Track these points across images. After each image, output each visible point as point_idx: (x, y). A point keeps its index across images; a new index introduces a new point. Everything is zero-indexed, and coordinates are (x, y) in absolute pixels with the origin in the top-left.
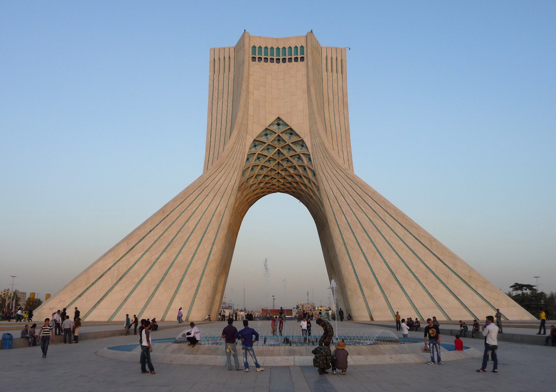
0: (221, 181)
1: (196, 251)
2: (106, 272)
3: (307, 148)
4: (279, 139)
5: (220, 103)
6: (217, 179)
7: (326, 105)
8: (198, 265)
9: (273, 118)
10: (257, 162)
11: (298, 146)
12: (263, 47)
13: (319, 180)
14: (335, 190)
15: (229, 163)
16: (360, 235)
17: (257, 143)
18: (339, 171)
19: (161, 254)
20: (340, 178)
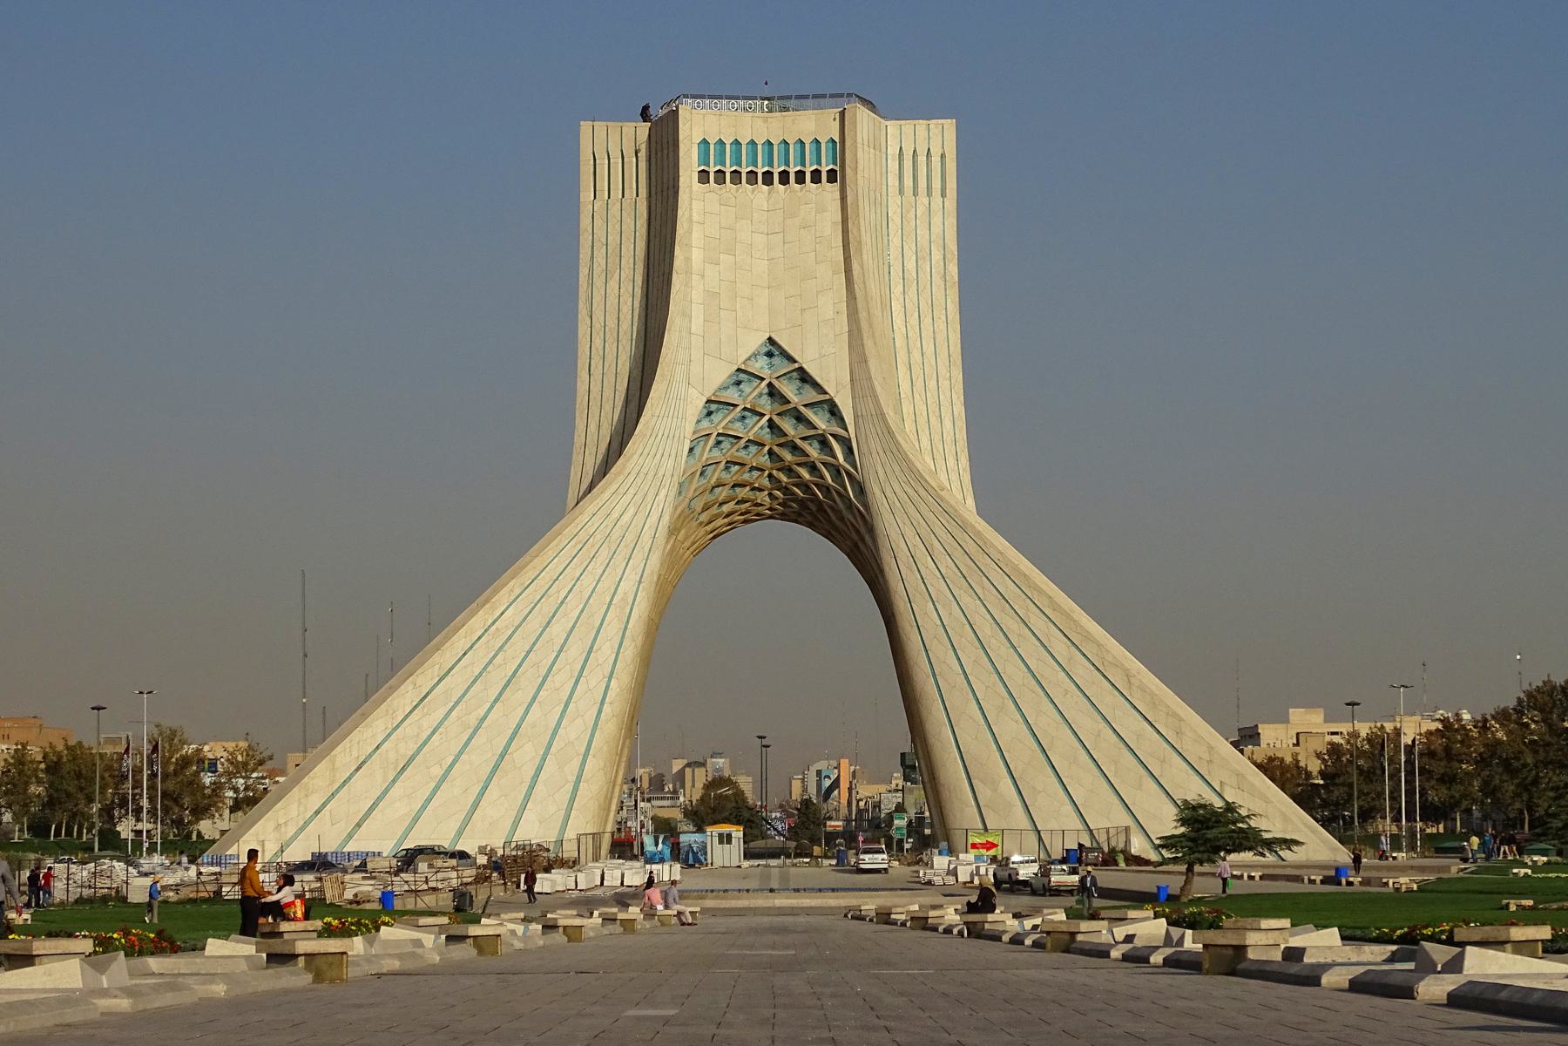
0: (626, 518)
1: (570, 697)
2: (370, 755)
3: (842, 419)
4: (773, 392)
5: (613, 284)
6: (615, 515)
7: (897, 290)
8: (575, 731)
9: (756, 341)
10: (716, 453)
11: (821, 412)
12: (728, 141)
13: (874, 509)
14: (914, 541)
15: (644, 470)
16: (970, 653)
17: (713, 407)
18: (922, 492)
19: (492, 707)
20: (923, 508)
